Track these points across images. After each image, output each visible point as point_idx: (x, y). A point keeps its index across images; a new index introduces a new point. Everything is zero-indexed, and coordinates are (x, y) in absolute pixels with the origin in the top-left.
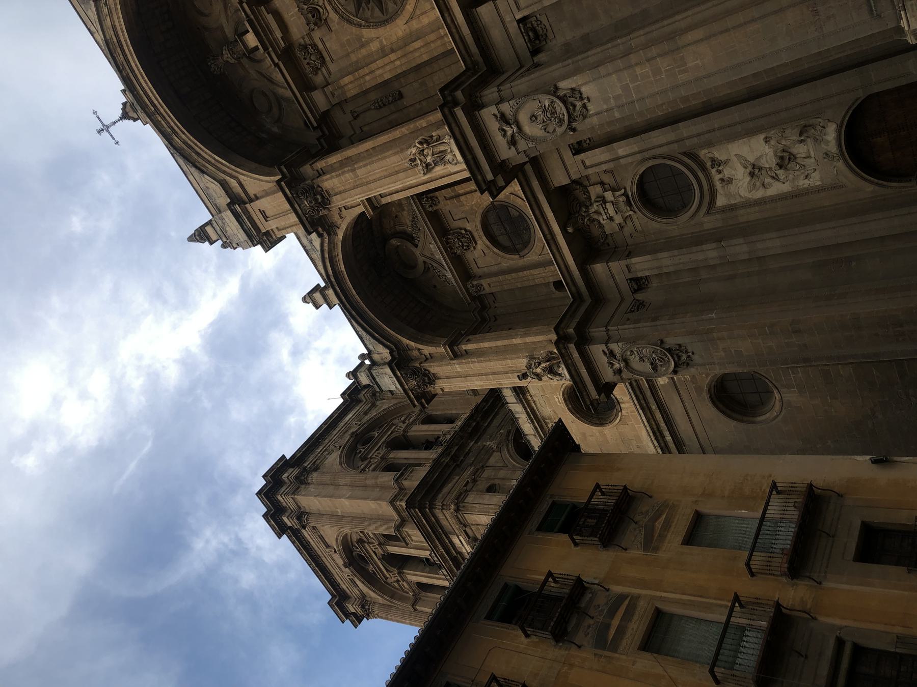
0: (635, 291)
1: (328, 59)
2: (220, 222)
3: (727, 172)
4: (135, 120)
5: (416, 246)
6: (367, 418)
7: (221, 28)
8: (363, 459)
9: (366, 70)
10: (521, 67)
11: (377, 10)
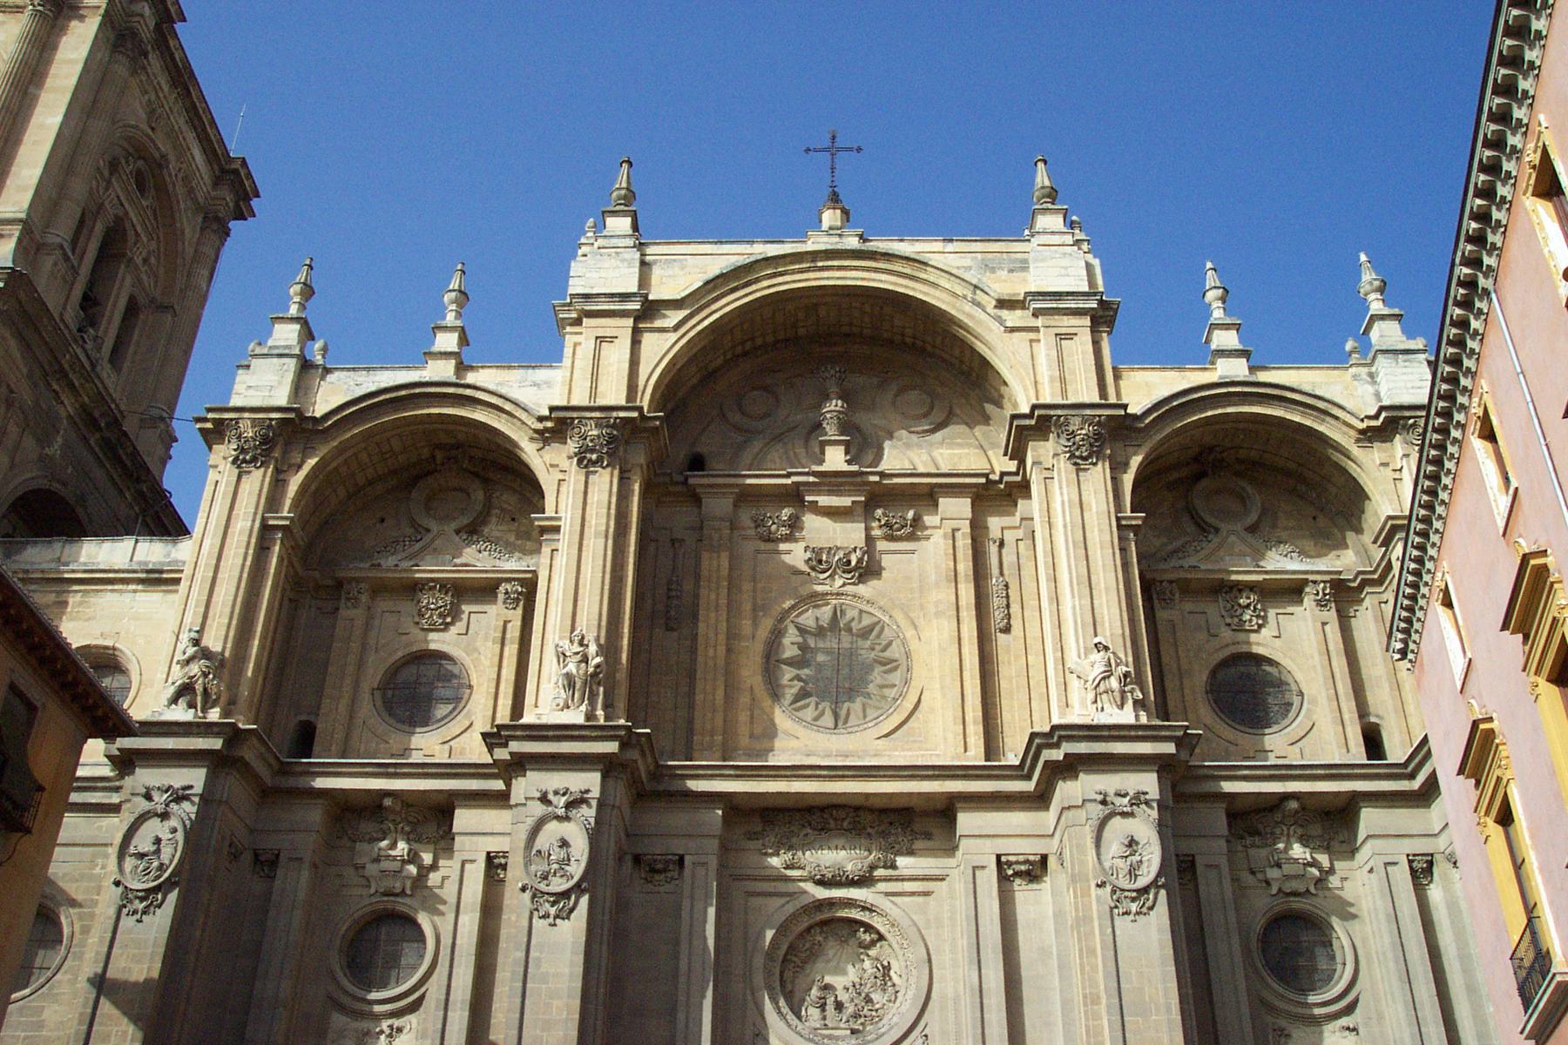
0: (256, 855)
1: (763, 546)
2: (627, 256)
5: (458, 532)
6: (180, 190)
8: (114, 166)
9: (723, 601)
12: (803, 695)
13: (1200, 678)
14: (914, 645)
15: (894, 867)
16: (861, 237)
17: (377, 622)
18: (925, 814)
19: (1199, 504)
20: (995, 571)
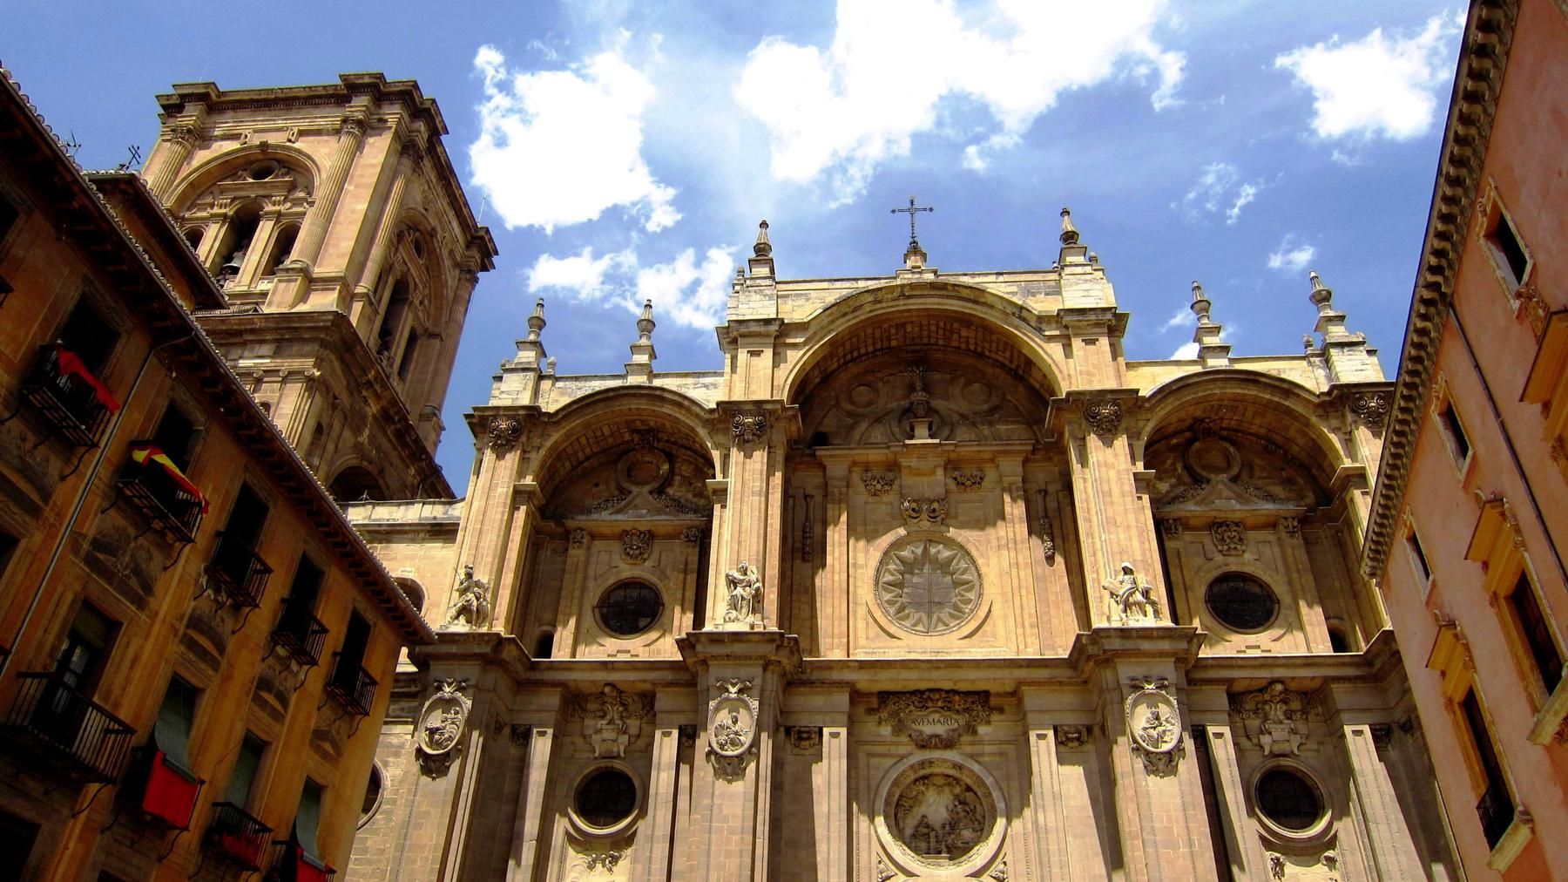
0: (514, 729)
3: (599, 866)
4: (906, 257)
6: (445, 253)
7: (946, 397)
10: (782, 712)
11: (888, 578)
12: (901, 609)
13: (1200, 591)
14: (983, 570)
15: (975, 732)
16: (935, 272)
17: (594, 559)
18: (998, 695)
19: (1192, 461)
20: (1041, 514)
